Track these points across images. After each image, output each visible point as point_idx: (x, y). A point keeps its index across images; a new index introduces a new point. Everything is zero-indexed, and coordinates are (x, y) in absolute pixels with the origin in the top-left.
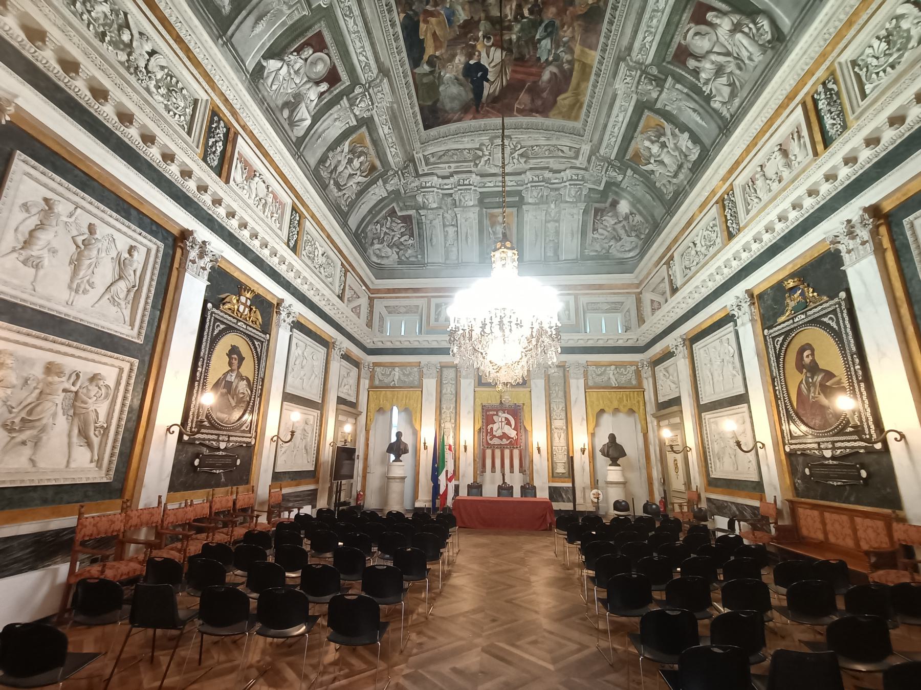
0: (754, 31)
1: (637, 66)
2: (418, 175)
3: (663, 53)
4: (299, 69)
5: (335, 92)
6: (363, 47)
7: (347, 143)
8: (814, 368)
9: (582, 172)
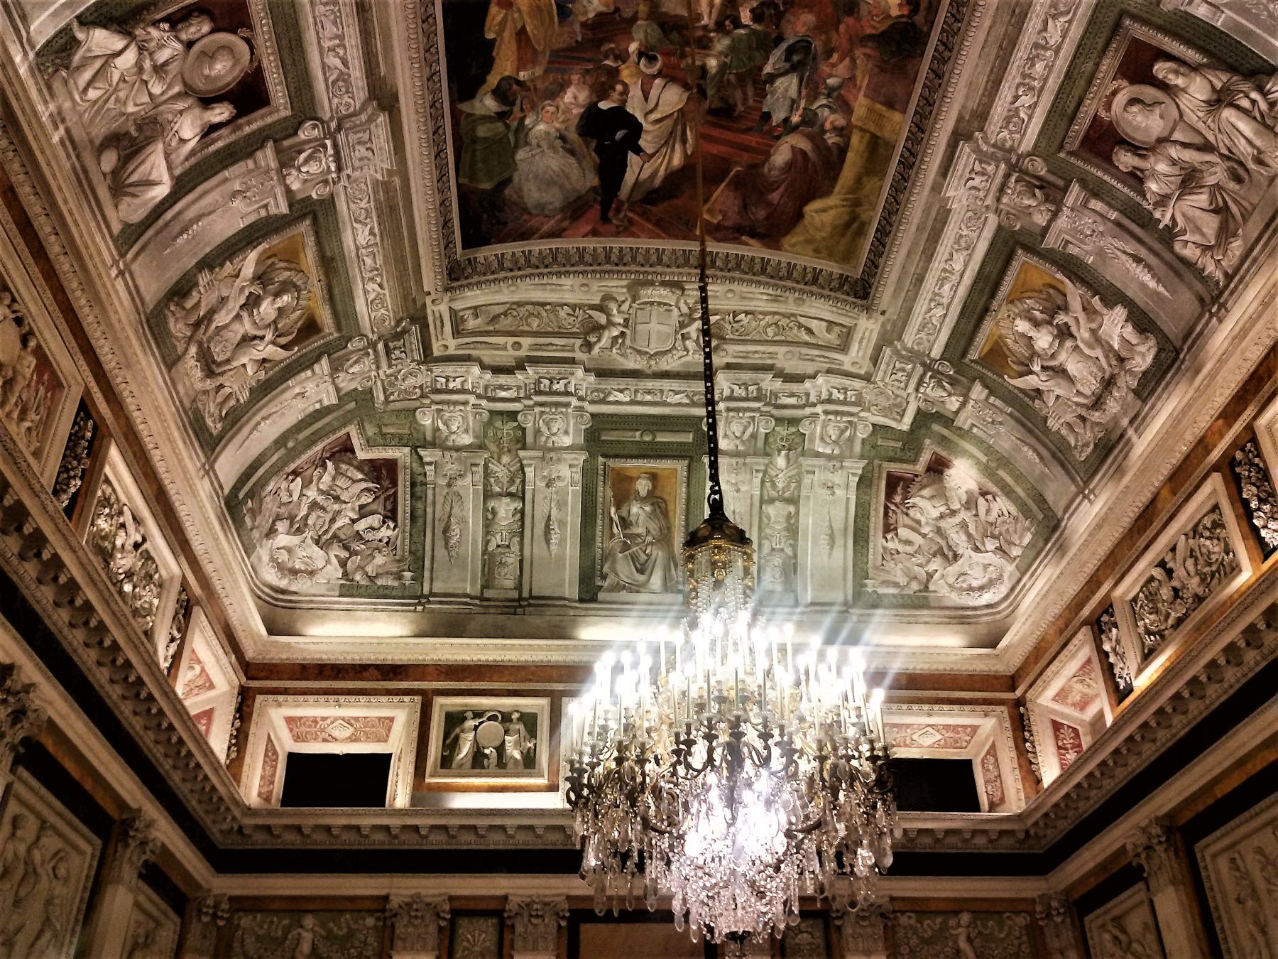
1: (1000, 154)
2: (427, 357)
3: (1062, 133)
4: (166, 63)
5: (247, 130)
6: (341, 37)
7: (253, 256)
9: (858, 384)
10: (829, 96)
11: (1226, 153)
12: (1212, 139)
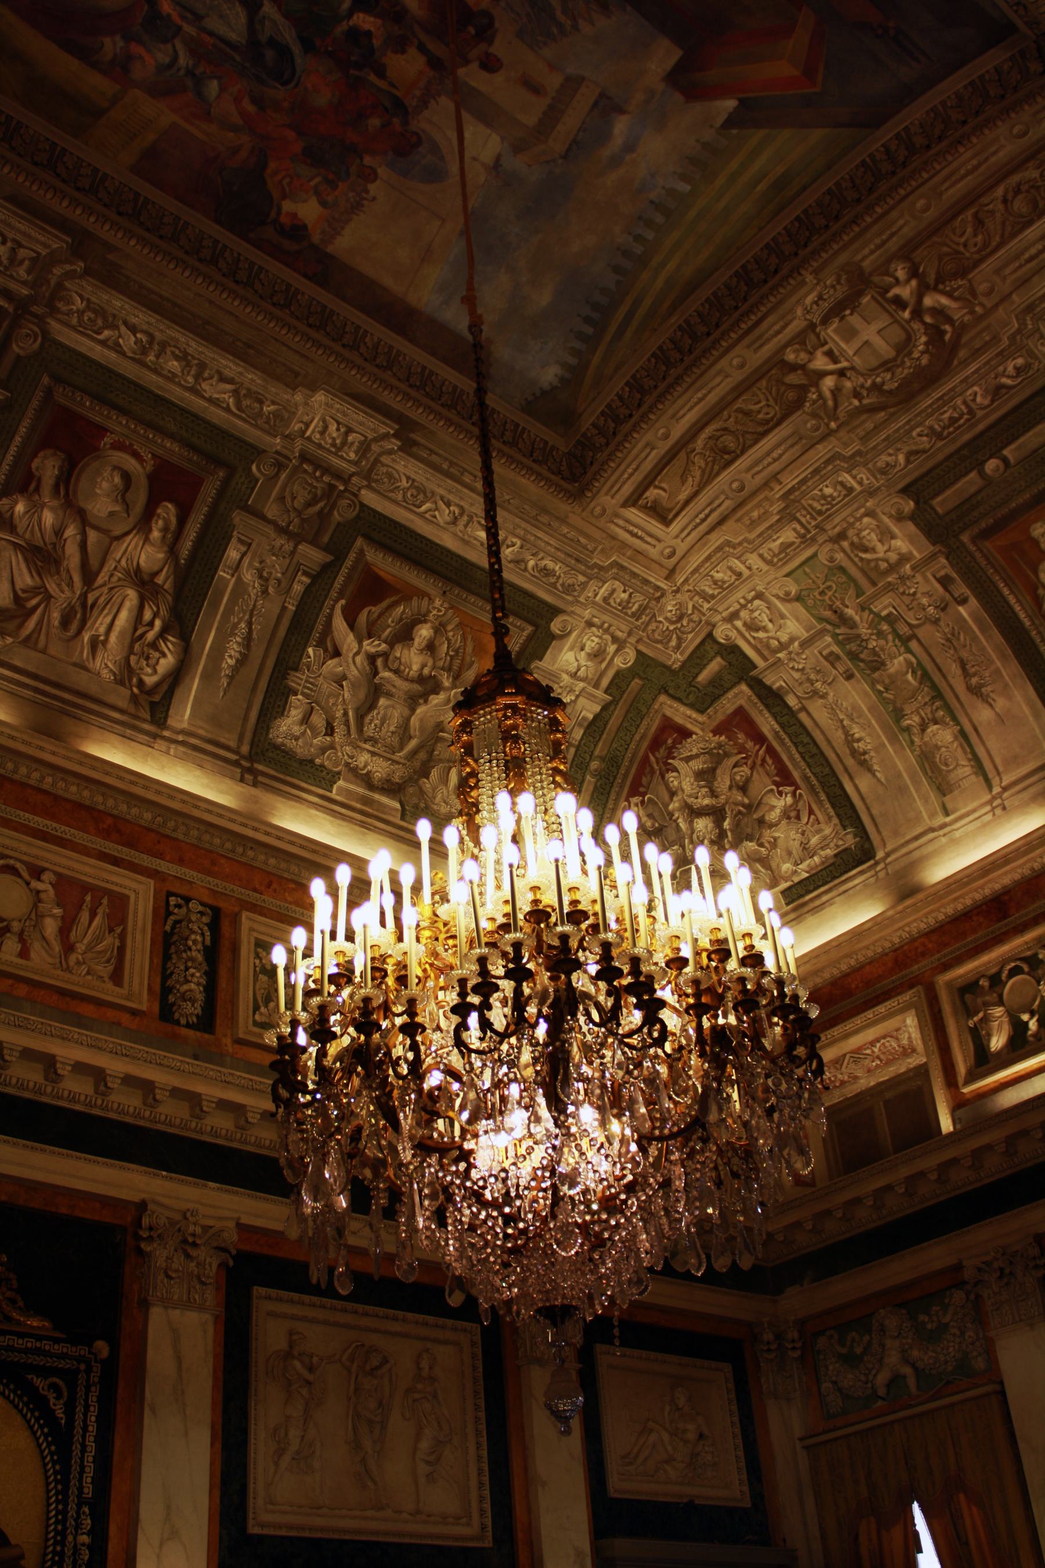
0: (151, 636)
10: (190, 73)
11: (90, 602)
12: (100, 581)
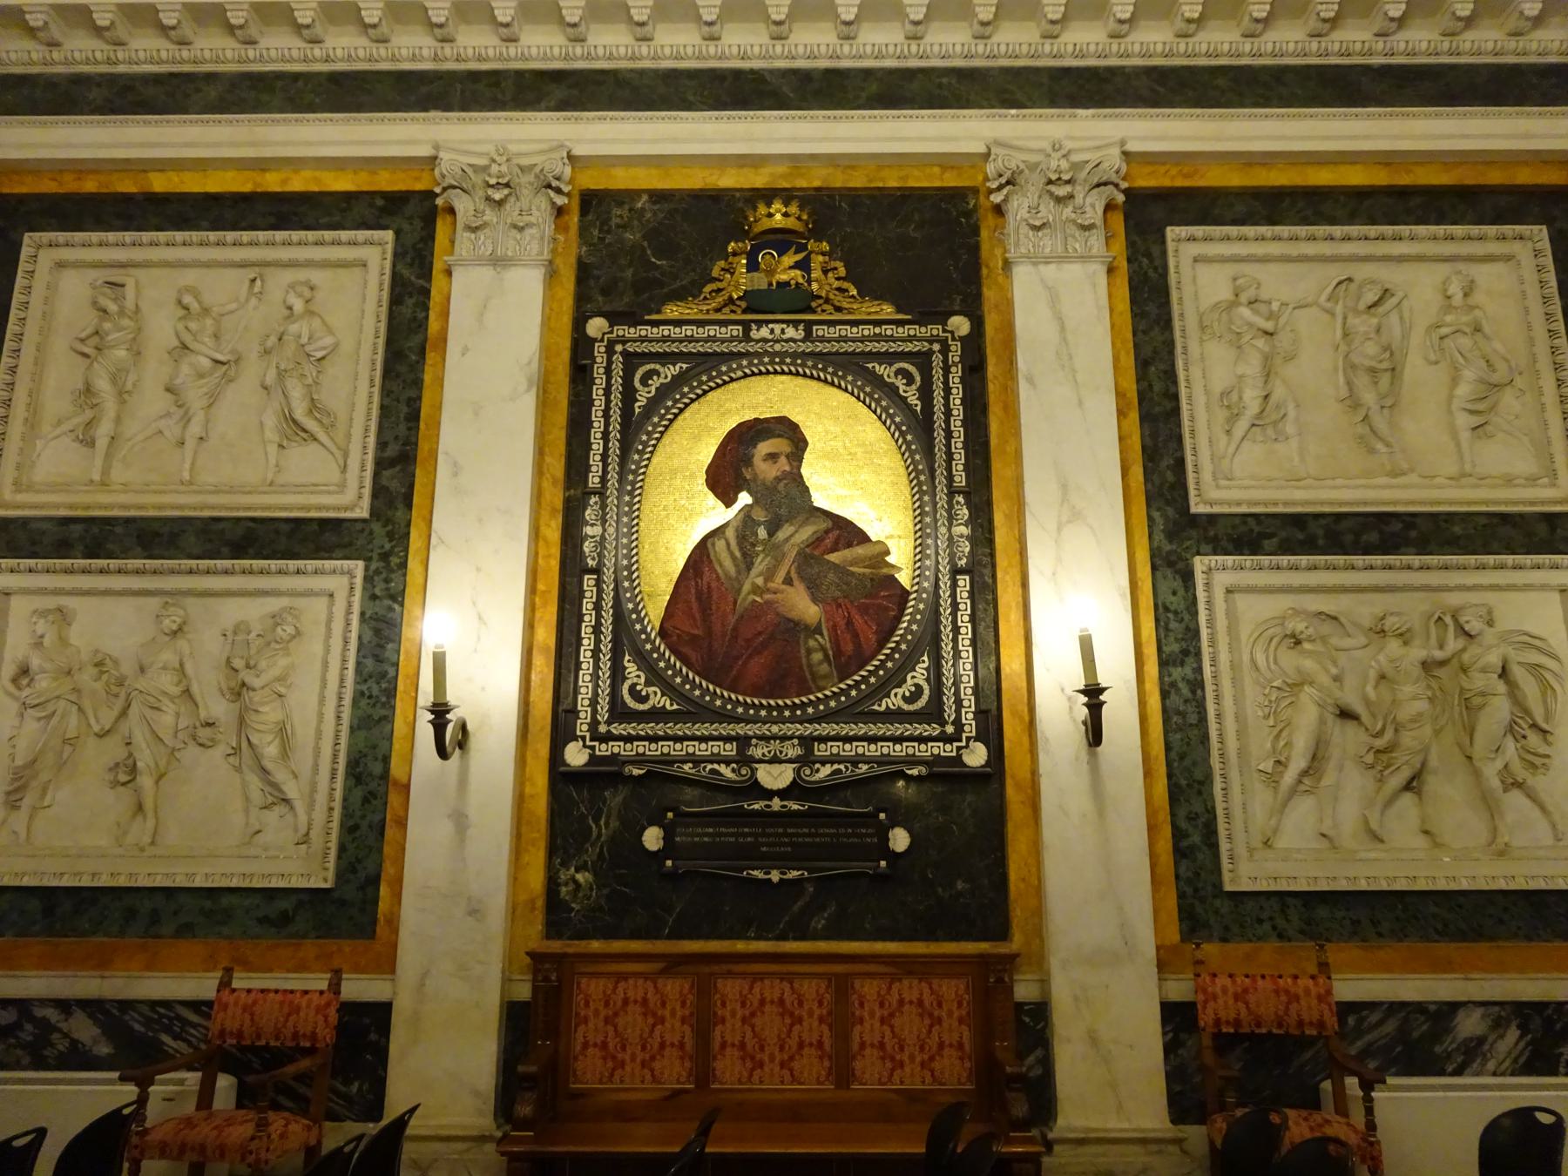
8: (788, 499)
